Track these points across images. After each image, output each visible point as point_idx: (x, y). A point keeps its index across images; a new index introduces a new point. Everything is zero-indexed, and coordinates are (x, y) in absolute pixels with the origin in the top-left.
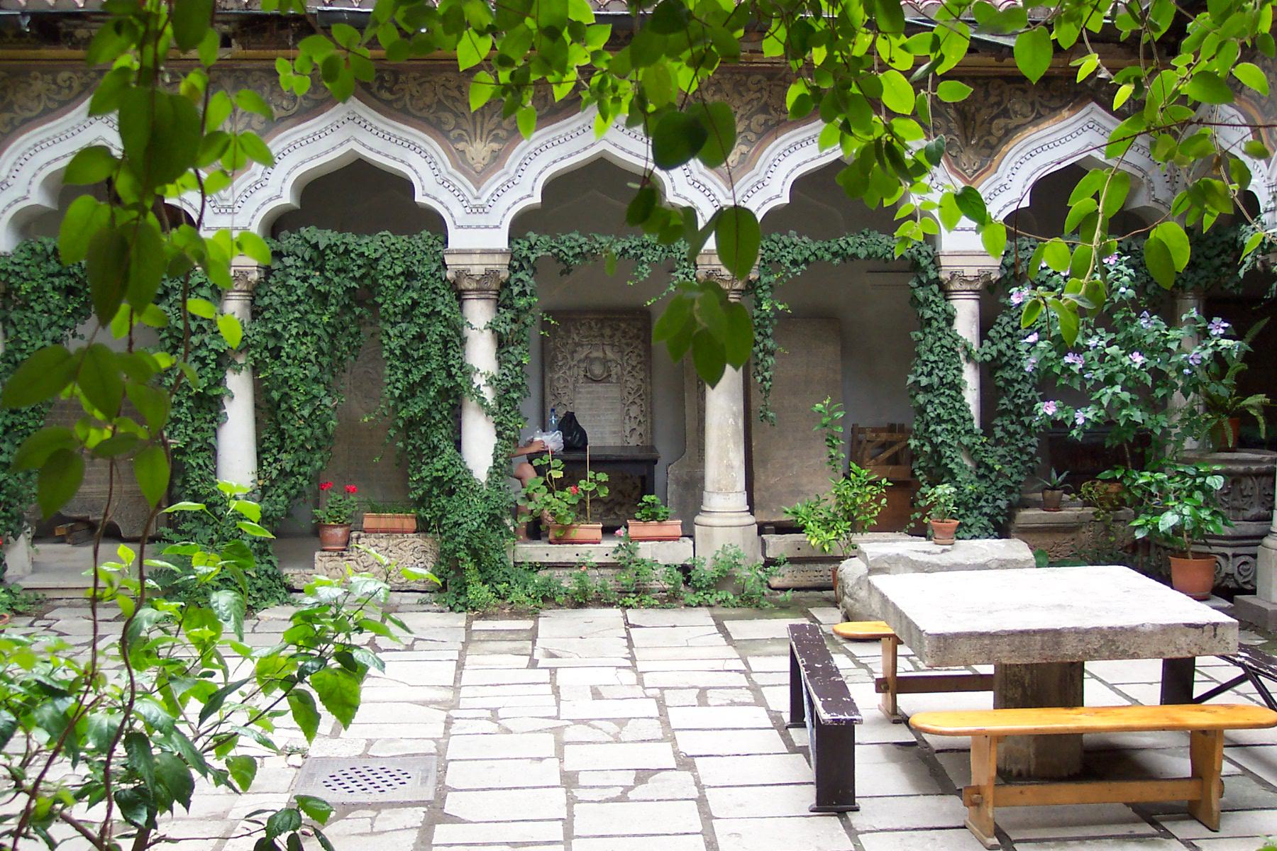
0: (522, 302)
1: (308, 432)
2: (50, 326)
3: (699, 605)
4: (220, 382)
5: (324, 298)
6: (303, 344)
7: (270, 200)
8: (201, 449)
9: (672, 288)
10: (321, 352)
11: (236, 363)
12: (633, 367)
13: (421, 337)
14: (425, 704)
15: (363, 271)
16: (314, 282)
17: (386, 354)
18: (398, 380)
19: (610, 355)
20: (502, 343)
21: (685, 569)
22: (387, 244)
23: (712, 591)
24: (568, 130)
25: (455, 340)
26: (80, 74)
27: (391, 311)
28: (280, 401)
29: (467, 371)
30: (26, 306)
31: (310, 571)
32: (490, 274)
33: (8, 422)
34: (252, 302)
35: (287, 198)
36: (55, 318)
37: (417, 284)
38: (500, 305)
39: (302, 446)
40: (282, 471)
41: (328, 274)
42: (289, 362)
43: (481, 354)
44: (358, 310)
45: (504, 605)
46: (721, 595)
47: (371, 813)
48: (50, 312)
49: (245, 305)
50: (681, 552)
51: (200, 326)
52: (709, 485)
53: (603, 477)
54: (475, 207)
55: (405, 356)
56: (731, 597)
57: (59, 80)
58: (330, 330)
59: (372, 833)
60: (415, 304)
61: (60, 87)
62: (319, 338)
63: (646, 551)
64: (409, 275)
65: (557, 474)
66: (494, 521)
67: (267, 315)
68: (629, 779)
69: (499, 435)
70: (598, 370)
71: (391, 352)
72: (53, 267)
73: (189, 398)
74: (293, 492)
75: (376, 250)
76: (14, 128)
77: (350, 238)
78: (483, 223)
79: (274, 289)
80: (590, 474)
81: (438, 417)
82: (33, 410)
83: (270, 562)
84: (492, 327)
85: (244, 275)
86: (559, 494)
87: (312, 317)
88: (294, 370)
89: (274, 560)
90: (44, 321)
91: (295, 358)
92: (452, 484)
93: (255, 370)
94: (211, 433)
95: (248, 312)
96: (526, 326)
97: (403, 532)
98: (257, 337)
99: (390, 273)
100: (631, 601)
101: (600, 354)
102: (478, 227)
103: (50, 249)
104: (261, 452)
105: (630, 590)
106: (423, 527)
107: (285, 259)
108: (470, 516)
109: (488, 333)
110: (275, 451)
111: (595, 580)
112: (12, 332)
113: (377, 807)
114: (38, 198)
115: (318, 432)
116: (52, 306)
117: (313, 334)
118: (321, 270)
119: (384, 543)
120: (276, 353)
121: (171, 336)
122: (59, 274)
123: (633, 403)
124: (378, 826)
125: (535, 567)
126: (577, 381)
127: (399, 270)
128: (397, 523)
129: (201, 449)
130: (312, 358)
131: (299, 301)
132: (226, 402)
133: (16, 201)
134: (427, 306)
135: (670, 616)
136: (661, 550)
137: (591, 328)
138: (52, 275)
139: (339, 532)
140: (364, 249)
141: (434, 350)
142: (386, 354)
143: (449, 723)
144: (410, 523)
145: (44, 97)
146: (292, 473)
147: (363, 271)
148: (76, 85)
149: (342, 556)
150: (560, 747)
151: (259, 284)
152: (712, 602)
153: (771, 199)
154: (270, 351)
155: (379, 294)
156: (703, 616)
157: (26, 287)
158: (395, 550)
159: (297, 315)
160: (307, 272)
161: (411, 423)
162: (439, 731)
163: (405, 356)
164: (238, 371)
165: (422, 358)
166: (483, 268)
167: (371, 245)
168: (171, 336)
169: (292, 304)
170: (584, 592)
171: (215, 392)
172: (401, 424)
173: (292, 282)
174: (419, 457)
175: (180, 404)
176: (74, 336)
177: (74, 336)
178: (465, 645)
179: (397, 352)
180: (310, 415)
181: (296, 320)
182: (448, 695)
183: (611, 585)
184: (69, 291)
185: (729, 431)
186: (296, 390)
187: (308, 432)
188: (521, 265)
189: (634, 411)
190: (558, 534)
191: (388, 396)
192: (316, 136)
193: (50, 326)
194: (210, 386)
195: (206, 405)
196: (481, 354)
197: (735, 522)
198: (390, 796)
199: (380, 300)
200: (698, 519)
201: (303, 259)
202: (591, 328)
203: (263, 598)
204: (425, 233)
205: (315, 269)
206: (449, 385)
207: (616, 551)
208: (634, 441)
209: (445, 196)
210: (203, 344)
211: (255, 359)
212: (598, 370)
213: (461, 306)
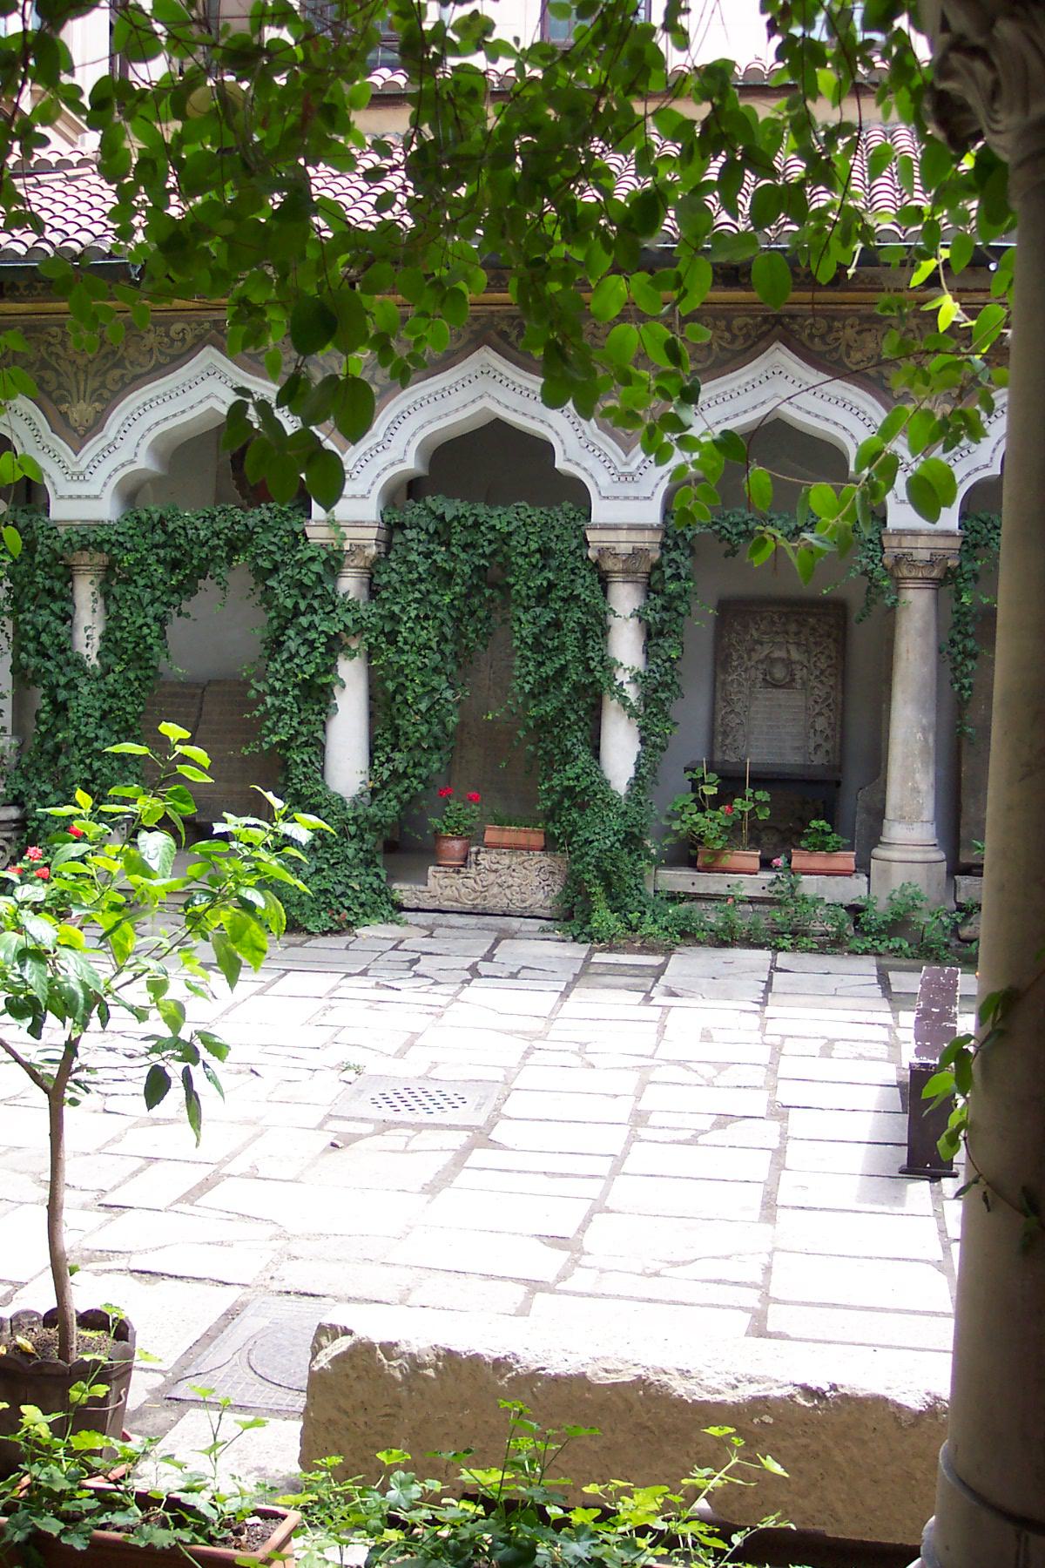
0: (672, 587)
1: (424, 729)
2: (152, 603)
3: (866, 952)
4: (330, 669)
5: (448, 577)
6: (423, 628)
7: (393, 464)
8: (306, 744)
10: (443, 638)
11: (349, 648)
12: (822, 672)
13: (556, 625)
14: (510, 1033)
15: (494, 546)
16: (438, 558)
17: (516, 643)
18: (529, 673)
19: (795, 656)
20: (652, 636)
21: (855, 910)
22: (523, 516)
23: (884, 937)
24: (734, 385)
25: (597, 628)
26: (194, 325)
27: (524, 593)
28: (395, 692)
29: (608, 665)
30: (129, 581)
31: (422, 888)
32: (636, 553)
33: (105, 706)
34: (371, 580)
35: (411, 464)
36: (158, 593)
37: (554, 563)
38: (650, 589)
39: (418, 745)
40: (394, 772)
41: (454, 550)
42: (407, 648)
43: (626, 646)
44: (488, 592)
45: (632, 937)
46: (895, 943)
47: (410, 1132)
48: (153, 587)
49: (362, 584)
50: (853, 889)
51: (310, 606)
52: (890, 813)
53: (763, 796)
55: (537, 646)
56: (906, 945)
57: (172, 333)
58: (454, 614)
59: (404, 1151)
60: (551, 586)
61: (173, 340)
62: (442, 623)
63: (810, 886)
64: (545, 552)
65: (711, 791)
66: (632, 841)
67: (384, 595)
68: (706, 1123)
69: (643, 741)
70: (779, 673)
71: (522, 640)
72: (159, 537)
73: (295, 685)
74: (406, 796)
75: (509, 523)
76: (125, 385)
77: (481, 509)
78: (632, 493)
79: (393, 565)
80: (749, 792)
81: (573, 717)
82: (132, 694)
83: (377, 875)
84: (639, 614)
85: (361, 548)
86: (710, 813)
87: (435, 598)
88: (411, 658)
89: (383, 873)
90: (147, 597)
91: (413, 644)
92: (587, 795)
93: (370, 656)
94: (319, 726)
95: (365, 591)
96: (680, 615)
97: (529, 849)
98: (373, 620)
99: (525, 549)
100: (786, 943)
101: (783, 654)
102: (627, 498)
103: (156, 517)
104: (373, 749)
105: (783, 931)
106: (550, 845)
107: (407, 532)
108: (602, 835)
109: (634, 621)
110: (388, 749)
111: (744, 918)
112: (113, 608)
113: (419, 1127)
114: (144, 462)
115: (436, 729)
116: (155, 580)
117: (435, 618)
118: (448, 545)
119: (506, 861)
120: (392, 637)
121: (279, 616)
122: (163, 546)
123: (820, 714)
124: (413, 1145)
125: (674, 898)
126: (753, 686)
127: (534, 546)
128: (521, 839)
129: (306, 744)
130: (434, 645)
131: (421, 580)
132: (336, 689)
133: (123, 465)
134: (565, 588)
135: (829, 962)
136: (827, 885)
137: (773, 623)
138: (156, 546)
139: (457, 845)
140: (495, 522)
141: (570, 640)
142: (516, 643)
143: (527, 1054)
144: (538, 839)
145: (156, 352)
146: (405, 775)
147: (494, 546)
148: (189, 337)
149: (458, 872)
150: (644, 1084)
151: (377, 561)
152: (881, 949)
153: (977, 470)
154: (385, 635)
155: (512, 573)
156: (868, 965)
157: (129, 558)
158: (518, 868)
159: (417, 595)
160: (431, 547)
161: (543, 724)
162: (513, 1059)
163: (537, 646)
164: (352, 657)
165: (557, 648)
166: (630, 546)
167: (502, 518)
168: (279, 616)
169: (413, 583)
170: (730, 929)
171: (324, 680)
172: (531, 724)
173: (413, 557)
174: (551, 763)
175: (286, 692)
176: (179, 614)
177: (179, 614)
178: (577, 977)
179: (530, 641)
180: (429, 710)
181: (415, 600)
182: (538, 1025)
183: (763, 923)
184: (175, 565)
185: (916, 748)
186: (412, 680)
187: (424, 729)
188: (676, 545)
189: (821, 723)
190: (708, 860)
191: (517, 690)
192: (445, 392)
193: (152, 603)
194: (317, 674)
195: (314, 695)
196: (626, 646)
197: (919, 857)
198: (438, 1117)
199: (512, 580)
200: (877, 852)
201: (427, 532)
202: (773, 623)
203: (365, 914)
204: (567, 505)
205: (441, 544)
206: (587, 680)
207: (772, 884)
208: (818, 759)
209: (590, 462)
210: (312, 626)
211: (370, 644)
212: (779, 673)
213: (605, 591)
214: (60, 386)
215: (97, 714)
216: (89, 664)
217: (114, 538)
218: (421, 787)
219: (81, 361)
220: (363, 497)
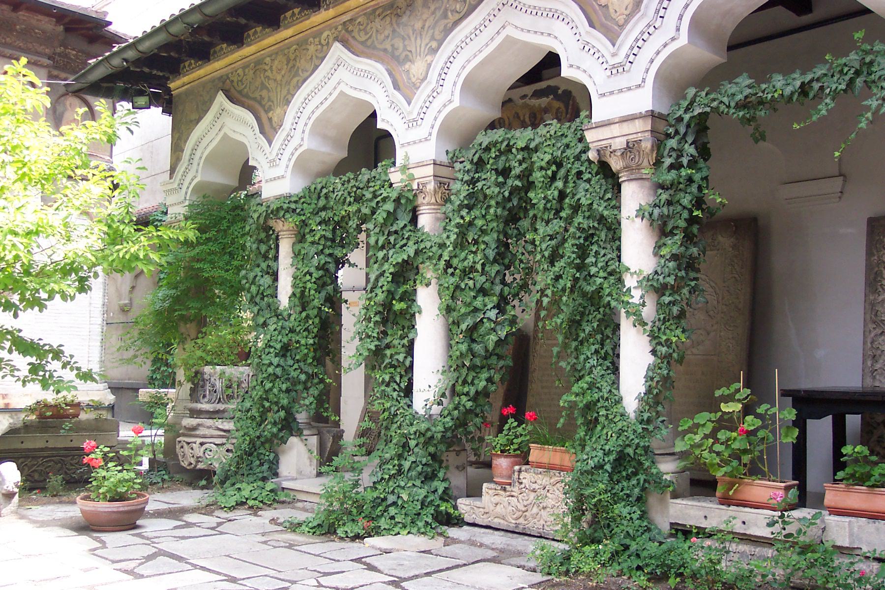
9: (863, 125)
31: (478, 503)
33: (285, 340)
54: (613, 66)
145: (314, 57)
149: (505, 490)
166: (623, 140)
196: (638, 251)
214: (269, 100)
215: (278, 346)
216: (281, 308)
217: (285, 206)
218: (469, 404)
219: (279, 78)
220: (426, 139)
